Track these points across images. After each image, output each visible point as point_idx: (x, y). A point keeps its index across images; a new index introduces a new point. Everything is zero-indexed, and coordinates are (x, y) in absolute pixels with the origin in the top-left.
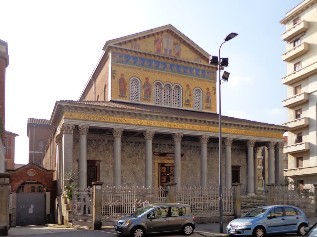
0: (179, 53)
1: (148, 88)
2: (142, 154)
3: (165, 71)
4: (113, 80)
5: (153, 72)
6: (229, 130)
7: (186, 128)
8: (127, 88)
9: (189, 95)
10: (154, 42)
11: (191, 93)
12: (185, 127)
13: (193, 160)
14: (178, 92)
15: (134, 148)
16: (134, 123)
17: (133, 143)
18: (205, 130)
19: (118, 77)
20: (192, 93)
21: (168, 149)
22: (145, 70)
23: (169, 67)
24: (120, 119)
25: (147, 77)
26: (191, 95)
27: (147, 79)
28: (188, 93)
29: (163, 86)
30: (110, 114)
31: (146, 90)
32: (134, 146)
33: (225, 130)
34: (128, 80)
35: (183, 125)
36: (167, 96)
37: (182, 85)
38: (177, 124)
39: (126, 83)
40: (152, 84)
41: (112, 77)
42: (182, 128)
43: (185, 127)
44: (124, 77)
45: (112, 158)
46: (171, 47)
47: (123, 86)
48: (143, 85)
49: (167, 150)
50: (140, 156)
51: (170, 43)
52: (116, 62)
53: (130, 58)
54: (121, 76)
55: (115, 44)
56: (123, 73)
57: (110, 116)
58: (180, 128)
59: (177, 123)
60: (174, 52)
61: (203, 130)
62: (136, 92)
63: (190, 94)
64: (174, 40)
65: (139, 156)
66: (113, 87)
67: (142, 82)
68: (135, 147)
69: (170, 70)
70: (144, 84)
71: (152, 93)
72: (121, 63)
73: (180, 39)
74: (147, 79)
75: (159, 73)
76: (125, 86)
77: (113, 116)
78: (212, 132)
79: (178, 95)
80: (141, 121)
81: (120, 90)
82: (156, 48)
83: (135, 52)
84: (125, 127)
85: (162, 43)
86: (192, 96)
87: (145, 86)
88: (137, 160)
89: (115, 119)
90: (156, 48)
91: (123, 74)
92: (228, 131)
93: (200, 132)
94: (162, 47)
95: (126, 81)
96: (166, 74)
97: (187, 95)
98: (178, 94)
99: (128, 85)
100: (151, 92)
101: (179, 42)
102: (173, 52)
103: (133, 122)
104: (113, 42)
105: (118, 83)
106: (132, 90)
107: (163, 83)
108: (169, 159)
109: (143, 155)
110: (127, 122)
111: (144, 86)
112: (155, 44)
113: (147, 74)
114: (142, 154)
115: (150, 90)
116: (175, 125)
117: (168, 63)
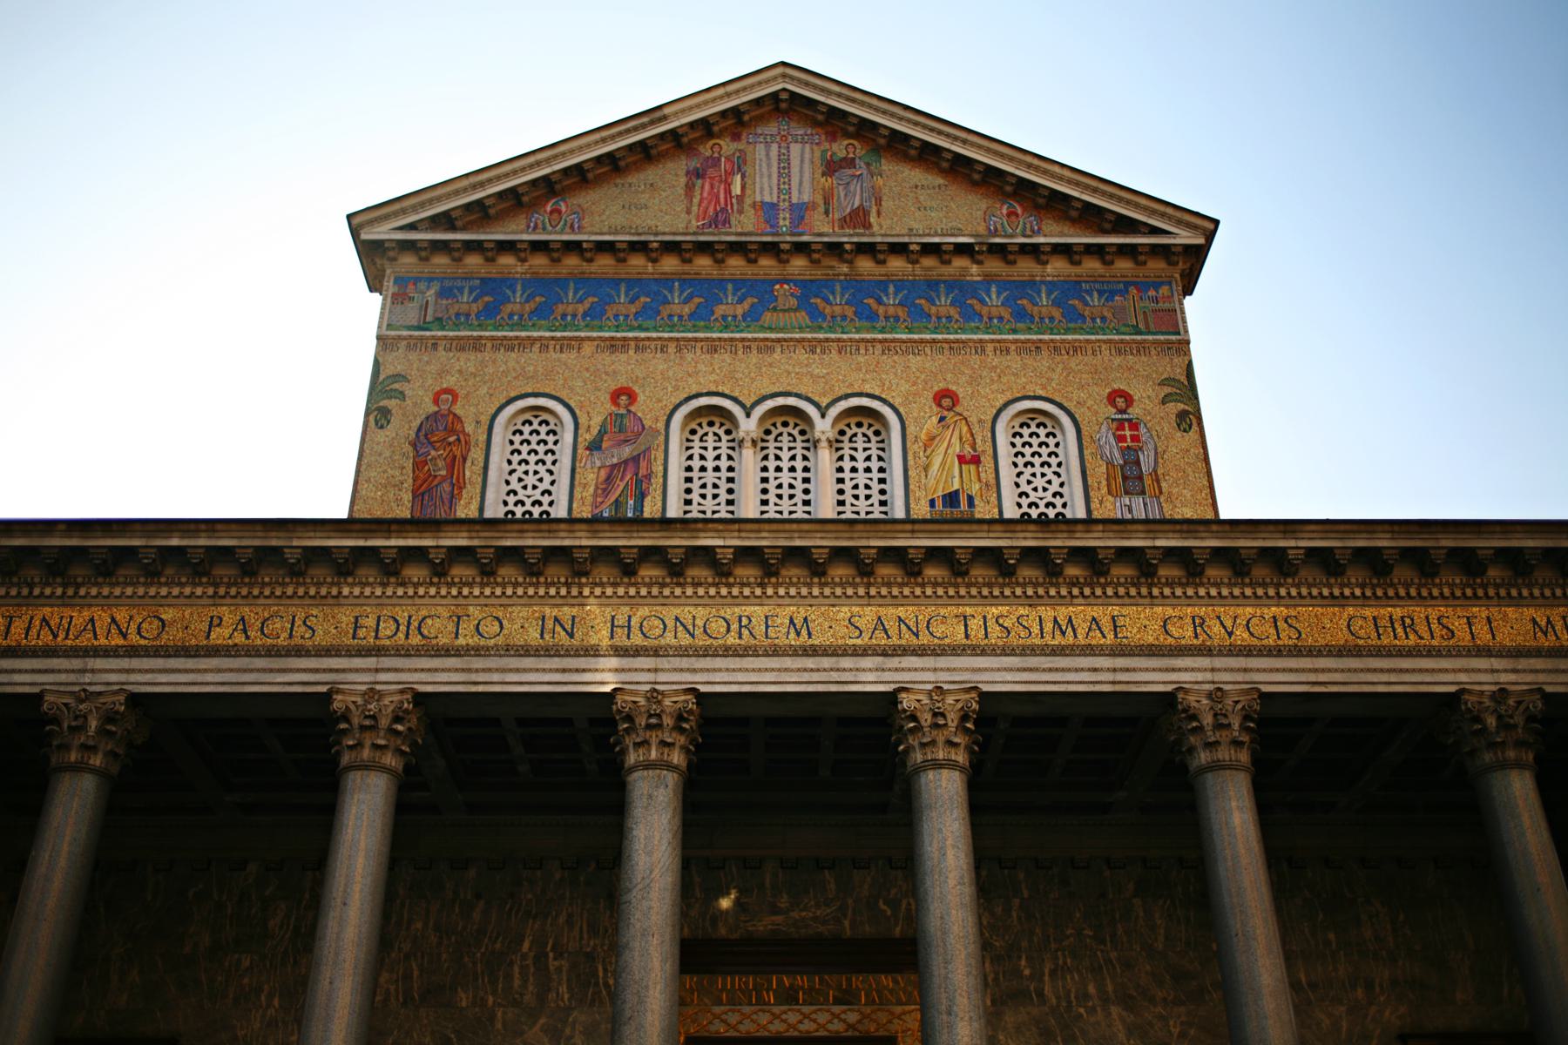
0: (866, 213)
1: (627, 451)
2: (540, 958)
3: (764, 329)
4: (380, 436)
5: (672, 348)
6: (1199, 623)
7: (732, 640)
8: (471, 472)
9: (962, 459)
10: (683, 180)
11: (973, 446)
12: (718, 627)
13: (1040, 994)
14: (874, 453)
15: (477, 915)
16: (239, 638)
17: (472, 873)
18: (925, 639)
19: (419, 403)
20: (983, 446)
21: (784, 902)
22: (614, 346)
23: (793, 302)
24: (121, 615)
25: (623, 382)
26: (976, 460)
27: (623, 395)
28: (952, 444)
29: (749, 426)
30: (31, 586)
31: (613, 466)
32: (478, 896)
33: (1156, 625)
34: (485, 419)
35: (701, 612)
36: (785, 491)
37: (897, 402)
38: (644, 611)
39: (465, 442)
40: (661, 426)
41: (372, 418)
42: (685, 640)
43: (718, 627)
44: (458, 410)
45: (271, 1012)
46: (805, 182)
47: (441, 463)
48: (586, 437)
49: (775, 911)
50: (525, 981)
51: (795, 170)
52: (409, 328)
53: (509, 292)
54: (436, 401)
55: (412, 227)
56: (450, 381)
57: (30, 601)
58: (669, 639)
59: (633, 602)
60: (827, 213)
61: (908, 639)
62: (537, 495)
63: (968, 450)
64: (826, 145)
65: (517, 982)
66: (368, 481)
67: (582, 420)
68: (482, 903)
69: (802, 317)
70: (595, 431)
71: (657, 481)
72: (443, 328)
73: (865, 129)
74: (624, 399)
75: (713, 347)
76: (455, 464)
77: (64, 601)
78: (1007, 651)
79: (875, 475)
80: (300, 615)
81: (414, 493)
82: (695, 209)
83: (538, 247)
84: (148, 677)
85: (738, 178)
86: (987, 461)
87: (604, 445)
88: (492, 1018)
89: (80, 618)
90: (695, 209)
91: (447, 391)
92: (1184, 633)
93: (868, 662)
94: (740, 199)
95: (469, 428)
96: (766, 346)
97: (943, 463)
98: (875, 465)
99: (476, 454)
100: (648, 477)
101: (859, 149)
102: (822, 209)
103: (227, 632)
104: (395, 214)
105: (408, 449)
106: (514, 479)
107: (742, 405)
108: (789, 997)
109: (553, 964)
110: (171, 637)
111: (595, 446)
112: (689, 189)
113: (624, 368)
114: (540, 958)
115: (643, 464)
116: (621, 620)
117: (782, 282)
